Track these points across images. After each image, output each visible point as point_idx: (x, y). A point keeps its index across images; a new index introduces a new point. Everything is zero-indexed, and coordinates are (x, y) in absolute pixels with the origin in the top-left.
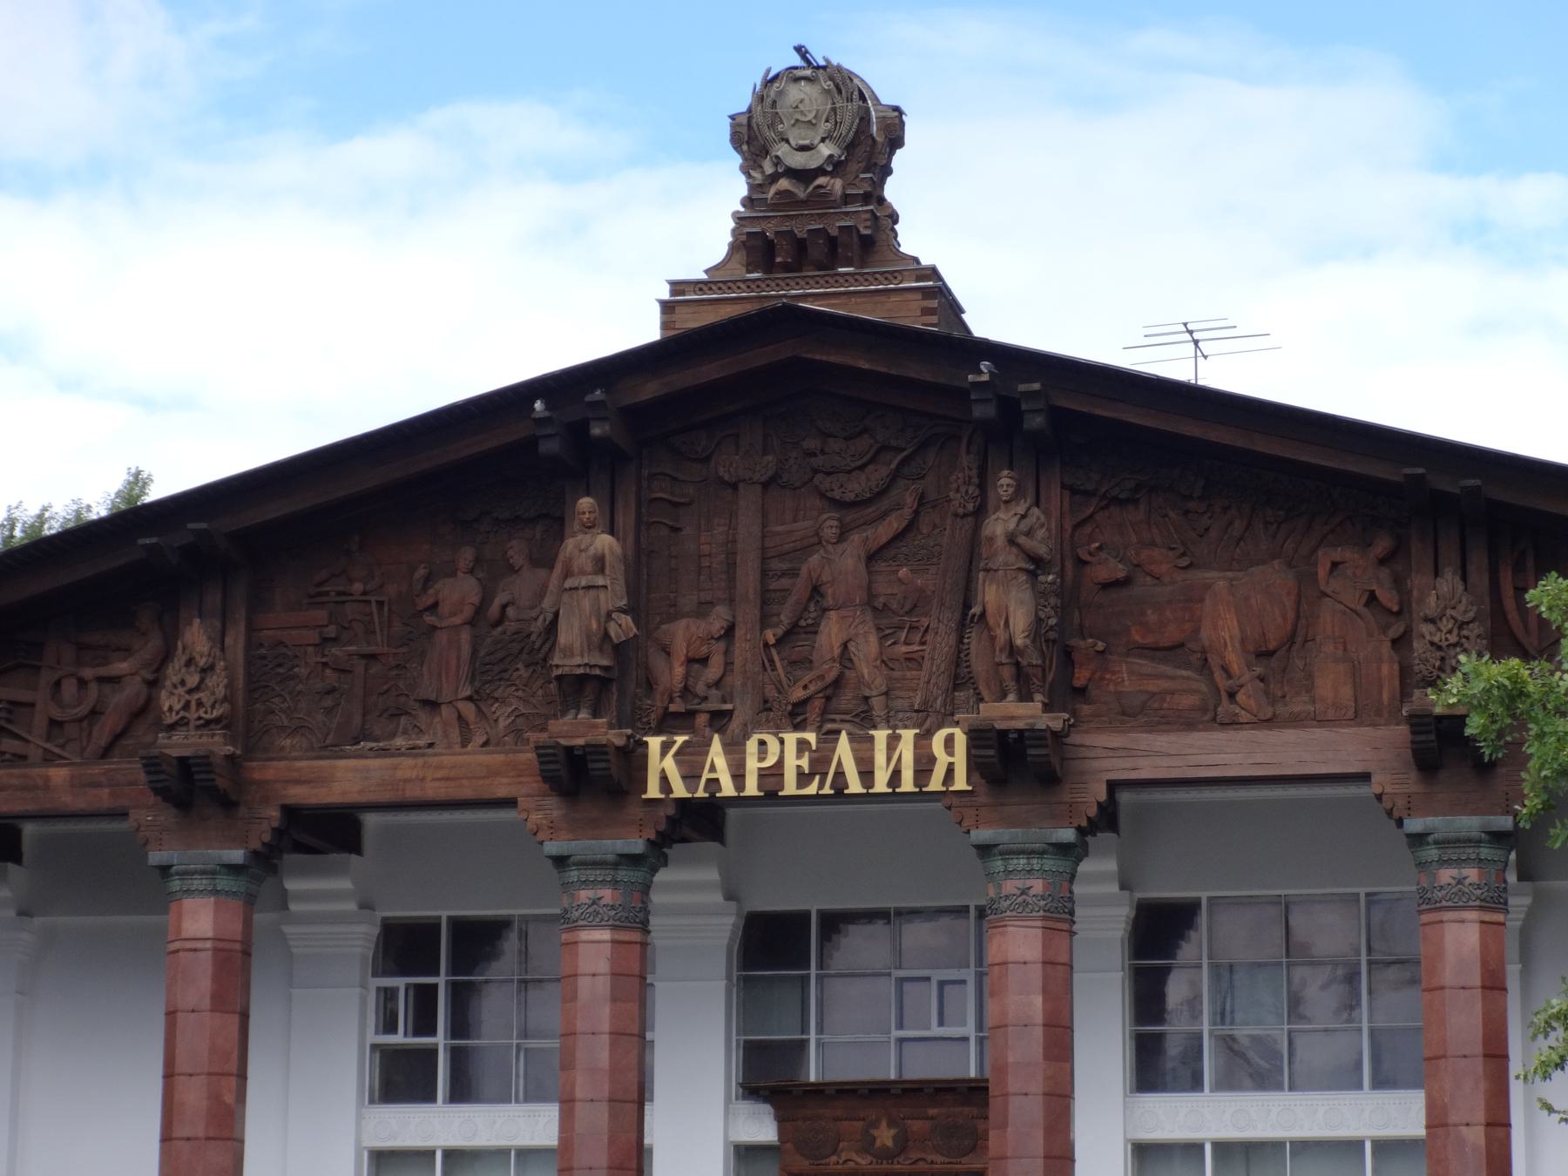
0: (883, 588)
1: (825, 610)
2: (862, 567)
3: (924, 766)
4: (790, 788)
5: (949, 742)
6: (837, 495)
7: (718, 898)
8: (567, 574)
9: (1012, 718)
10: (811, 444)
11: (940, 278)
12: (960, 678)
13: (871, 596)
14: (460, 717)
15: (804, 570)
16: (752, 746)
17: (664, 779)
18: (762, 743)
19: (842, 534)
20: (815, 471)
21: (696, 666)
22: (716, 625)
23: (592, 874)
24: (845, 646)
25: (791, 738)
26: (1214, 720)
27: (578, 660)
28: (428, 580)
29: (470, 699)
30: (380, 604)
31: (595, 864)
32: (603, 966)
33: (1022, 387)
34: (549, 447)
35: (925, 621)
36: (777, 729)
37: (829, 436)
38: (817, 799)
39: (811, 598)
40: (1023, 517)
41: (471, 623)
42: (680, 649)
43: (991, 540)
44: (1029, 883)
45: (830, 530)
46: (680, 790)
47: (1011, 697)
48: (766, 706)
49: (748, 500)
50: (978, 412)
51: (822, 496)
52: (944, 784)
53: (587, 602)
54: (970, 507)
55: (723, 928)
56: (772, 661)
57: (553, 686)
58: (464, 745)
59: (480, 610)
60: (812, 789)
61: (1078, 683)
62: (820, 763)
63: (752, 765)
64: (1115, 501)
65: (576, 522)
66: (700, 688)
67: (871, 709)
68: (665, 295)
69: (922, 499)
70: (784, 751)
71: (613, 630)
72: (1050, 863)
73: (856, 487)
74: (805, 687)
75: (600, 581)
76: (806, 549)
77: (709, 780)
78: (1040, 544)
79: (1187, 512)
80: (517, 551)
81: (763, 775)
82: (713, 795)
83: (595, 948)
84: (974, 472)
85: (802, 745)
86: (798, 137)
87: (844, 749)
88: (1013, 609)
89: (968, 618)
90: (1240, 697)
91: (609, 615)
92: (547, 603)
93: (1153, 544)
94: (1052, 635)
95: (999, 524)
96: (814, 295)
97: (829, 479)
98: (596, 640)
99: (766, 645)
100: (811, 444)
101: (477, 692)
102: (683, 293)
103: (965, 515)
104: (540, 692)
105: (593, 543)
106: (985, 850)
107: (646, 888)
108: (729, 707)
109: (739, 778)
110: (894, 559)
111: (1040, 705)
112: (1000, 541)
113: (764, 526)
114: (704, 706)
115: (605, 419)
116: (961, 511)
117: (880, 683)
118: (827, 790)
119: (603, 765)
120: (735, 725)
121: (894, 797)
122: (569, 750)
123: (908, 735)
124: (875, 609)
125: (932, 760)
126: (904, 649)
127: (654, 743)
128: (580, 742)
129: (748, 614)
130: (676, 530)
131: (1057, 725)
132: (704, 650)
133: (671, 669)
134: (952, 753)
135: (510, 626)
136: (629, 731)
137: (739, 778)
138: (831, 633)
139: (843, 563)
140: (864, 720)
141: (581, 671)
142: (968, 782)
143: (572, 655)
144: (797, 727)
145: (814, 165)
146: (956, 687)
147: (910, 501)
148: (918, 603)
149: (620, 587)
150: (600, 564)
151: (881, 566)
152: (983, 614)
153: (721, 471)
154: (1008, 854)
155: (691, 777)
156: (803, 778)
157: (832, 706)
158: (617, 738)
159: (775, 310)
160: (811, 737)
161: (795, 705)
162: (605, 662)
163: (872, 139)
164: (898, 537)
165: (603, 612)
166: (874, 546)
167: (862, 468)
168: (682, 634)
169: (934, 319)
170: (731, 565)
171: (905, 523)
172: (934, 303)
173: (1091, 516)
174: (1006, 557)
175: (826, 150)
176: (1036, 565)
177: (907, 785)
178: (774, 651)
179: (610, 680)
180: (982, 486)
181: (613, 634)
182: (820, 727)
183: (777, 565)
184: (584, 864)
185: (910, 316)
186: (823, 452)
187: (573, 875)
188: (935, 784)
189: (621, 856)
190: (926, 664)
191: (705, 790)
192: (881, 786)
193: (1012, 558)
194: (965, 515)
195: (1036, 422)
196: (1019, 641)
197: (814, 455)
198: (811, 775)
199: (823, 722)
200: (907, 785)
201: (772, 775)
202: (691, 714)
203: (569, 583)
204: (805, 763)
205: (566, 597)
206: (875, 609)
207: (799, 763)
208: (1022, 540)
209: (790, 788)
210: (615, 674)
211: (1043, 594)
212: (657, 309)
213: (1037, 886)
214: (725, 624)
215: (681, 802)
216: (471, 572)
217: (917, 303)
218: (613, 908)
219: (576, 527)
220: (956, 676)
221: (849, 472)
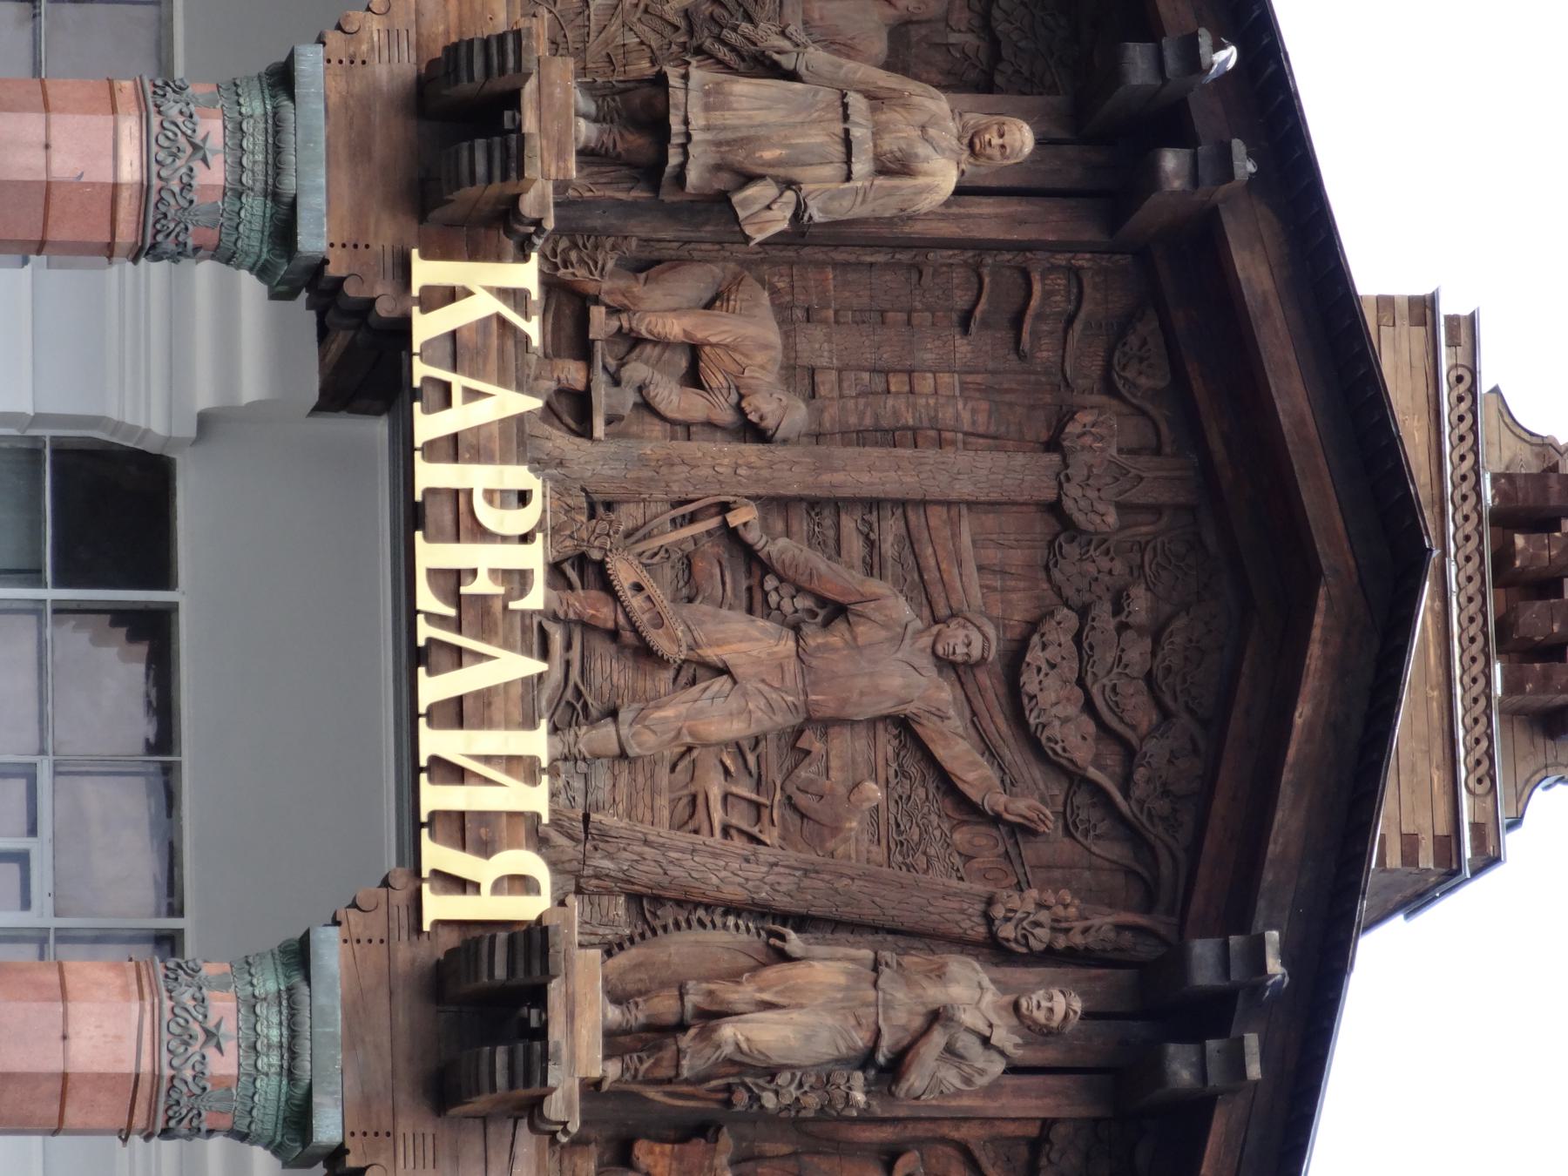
0: (844, 748)
1: (796, 628)
2: (886, 707)
3: (465, 830)
4: (430, 554)
5: (521, 884)
6: (1035, 656)
7: (204, 398)
8: (876, 98)
9: (571, 1017)
10: (1140, 604)
11: (1476, 872)
12: (653, 907)
13: (827, 725)
15: (875, 586)
16: (518, 476)
17: (451, 295)
18: (523, 498)
19: (954, 665)
20: (1083, 612)
21: (683, 363)
22: (768, 405)
23: (255, 143)
24: (722, 670)
25: (533, 558)
27: (697, 120)
31: (276, 150)
32: (64, 166)
33: (1252, 1041)
34: (1138, 64)
35: (771, 836)
36: (551, 528)
37: (1156, 642)
38: (408, 611)
39: (822, 601)
40: (986, 1041)
42: (716, 329)
43: (939, 974)
44: (230, 1046)
45: (962, 641)
46: (426, 327)
47: (614, 1014)
48: (599, 506)
50: (1203, 951)
51: (1033, 626)
52: (436, 873)
53: (820, 138)
54: (1007, 931)
55: (139, 411)
56: (692, 518)
57: (643, 67)
60: (427, 599)
61: (641, 1150)
62: (474, 614)
63: (474, 477)
65: (983, 119)
66: (636, 371)
69: (1022, 831)
70: (505, 542)
71: (759, 192)
72: (270, 1089)
73: (1051, 694)
74: (638, 588)
75: (861, 166)
76: (922, 590)
77: (446, 387)
78: (928, 1075)
81: (458, 498)
82: (416, 395)
83: (106, 149)
84: (1078, 940)
85: (518, 580)
87: (508, 666)
88: (799, 1017)
89: (778, 926)
91: (789, 184)
92: (817, 57)
94: (741, 1099)
95: (971, 991)
96: (1449, 613)
97: (1067, 640)
98: (739, 157)
99: (725, 508)
102: (1453, 342)
103: (989, 920)
104: (632, 40)
105: (942, 152)
106: (299, 956)
107: (226, 256)
108: (599, 429)
109: (453, 448)
110: (902, 773)
111: (596, 1073)
112: (935, 994)
113: (971, 505)
114: (600, 378)
115: (1195, 179)
116: (998, 912)
117: (643, 742)
118: (424, 631)
119: (481, 169)
120: (560, 441)
121: (411, 769)
122: (512, 99)
123: (536, 799)
124: (798, 732)
125: (486, 849)
126: (715, 793)
127: (526, 275)
128: (530, 124)
129: (791, 471)
131: (555, 1108)
132: (716, 379)
134: (500, 889)
136: (550, 224)
137: (453, 448)
138: (749, 642)
139: (891, 666)
140: (571, 709)
141: (676, 125)
142: (439, 923)
143: (707, 108)
144: (555, 570)
146: (635, 899)
147: (1021, 807)
149: (846, 208)
150: (895, 167)
151: (887, 743)
152: (784, 957)
153: (1085, 418)
154: (290, 1002)
155: (454, 348)
156: (451, 581)
157: (599, 636)
158: (537, 199)
159: (1415, 533)
160: (536, 599)
161: (601, 566)
162: (693, 176)
164: (946, 782)
165: (796, 173)
167: (1089, 707)
168: (750, 334)
169: (1394, 860)
170: (889, 436)
171: (974, 795)
172: (1426, 860)
174: (902, 1004)
176: (887, 1068)
177: (435, 797)
178: (713, 523)
179: (656, 187)
180: (1049, 956)
181: (752, 191)
182: (555, 617)
183: (890, 530)
184: (276, 126)
185: (1405, 808)
186: (1122, 627)
187: (255, 106)
188: (436, 855)
189: (293, 205)
190: (683, 838)
191: (427, 380)
192: (433, 742)
193: (900, 1017)
194: (989, 920)
195: (1181, 1067)
196: (728, 1031)
197: (1117, 610)
198: (457, 600)
199: (566, 623)
200: (435, 797)
202: (584, 351)
203: (856, 101)
204: (482, 586)
205: (827, 95)
206: (798, 732)
207: (483, 575)
208: (938, 1038)
209: (430, 554)
211: (826, 1082)
212: (1422, 290)
213: (224, 1064)
214: (769, 423)
215: (403, 328)
217: (1428, 823)
218: (186, 187)
219: (973, 119)
220: (658, 900)
221: (1081, 682)
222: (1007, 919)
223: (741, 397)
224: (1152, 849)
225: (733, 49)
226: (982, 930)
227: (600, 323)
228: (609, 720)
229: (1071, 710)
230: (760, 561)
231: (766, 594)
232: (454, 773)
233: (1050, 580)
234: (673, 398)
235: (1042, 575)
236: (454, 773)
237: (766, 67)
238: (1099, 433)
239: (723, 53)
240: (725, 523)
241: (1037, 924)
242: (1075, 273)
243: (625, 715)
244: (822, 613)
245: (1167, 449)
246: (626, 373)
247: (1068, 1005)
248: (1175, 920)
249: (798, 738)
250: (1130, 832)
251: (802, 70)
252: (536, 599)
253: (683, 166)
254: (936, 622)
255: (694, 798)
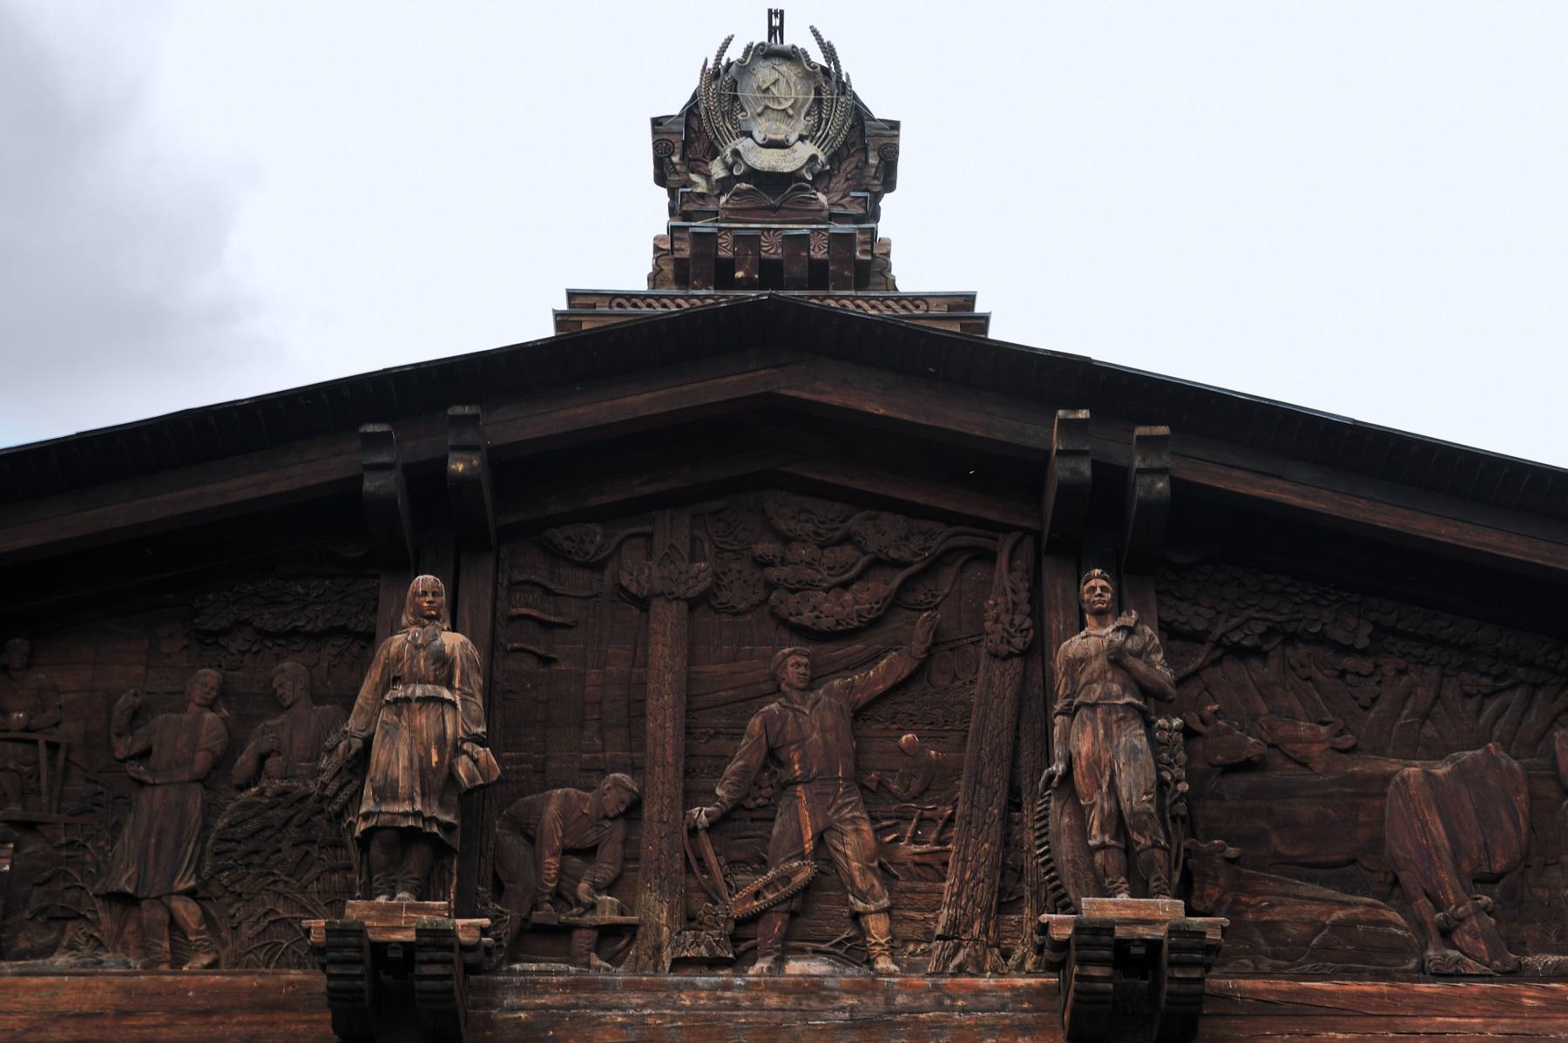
6: (807, 618)
10: (766, 548)
14: (173, 923)
19: (812, 680)
21: (575, 861)
24: (820, 839)
26: (1421, 968)
27: (406, 807)
28: (137, 716)
29: (191, 893)
30: (53, 747)
39: (765, 767)
41: (204, 781)
49: (667, 620)
51: (783, 622)
53: (424, 720)
54: (1019, 642)
58: (177, 963)
59: (222, 762)
64: (1240, 652)
67: (863, 933)
68: (563, 306)
71: (463, 768)
76: (756, 699)
79: (1343, 674)
80: (290, 673)
86: (762, 129)
90: (1462, 937)
93: (1293, 717)
97: (793, 599)
99: (693, 832)
100: (766, 548)
101: (205, 884)
103: (1010, 655)
104: (315, 886)
108: (634, 919)
116: (1004, 649)
124: (863, 787)
129: (664, 782)
130: (546, 661)
132: (590, 838)
133: (537, 862)
135: (273, 786)
139: (815, 721)
143: (395, 798)
145: (787, 167)
148: (935, 781)
153: (625, 580)
161: (742, 922)
162: (448, 818)
164: (899, 687)
166: (862, 698)
167: (845, 585)
170: (635, 711)
173: (1196, 673)
175: (806, 150)
179: (451, 851)
186: (784, 562)
194: (1010, 655)
197: (772, 564)
206: (863, 787)
210: (455, 842)
214: (626, 797)
216: (211, 707)
221: (827, 590)
222: (1009, 643)
223: (606, 817)
224: (949, 551)
225: (341, 789)
226: (1016, 661)
227: (546, 913)
228: (862, 920)
229: (848, 596)
230: (734, 809)
231: (759, 806)
233: (745, 613)
234: (606, 869)
235: (741, 619)
237: (363, 757)
238: (638, 571)
239: (343, 797)
240: (708, 830)
241: (1012, 624)
242: (514, 585)
243: (860, 906)
244: (773, 768)
245: (648, 529)
246: (586, 899)
247: (1098, 577)
248: (1001, 536)
249: (870, 790)
250: (932, 568)
251: (364, 734)
253: (440, 824)
254: (779, 690)
255: (917, 864)
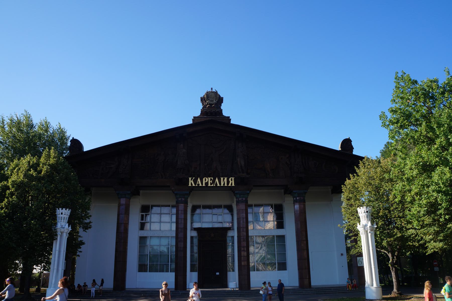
4: (209, 185)
5: (232, 179)
25: (209, 178)
60: (212, 185)
70: (209, 180)
85: (211, 179)
87: (217, 180)
121: (224, 186)
123: (226, 179)
127: (190, 178)
137: (202, 184)
155: (195, 184)
156: (211, 184)
157: (215, 175)
163: (220, 100)
177: (226, 185)
188: (230, 185)
192: (222, 185)
200: (226, 185)
201: (207, 184)
232: (224, 184)
236: (224, 184)
252: (212, 178)
